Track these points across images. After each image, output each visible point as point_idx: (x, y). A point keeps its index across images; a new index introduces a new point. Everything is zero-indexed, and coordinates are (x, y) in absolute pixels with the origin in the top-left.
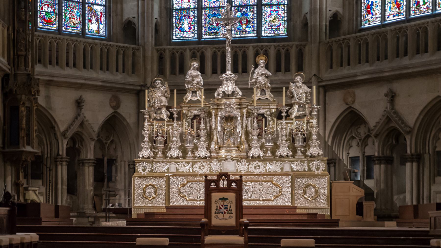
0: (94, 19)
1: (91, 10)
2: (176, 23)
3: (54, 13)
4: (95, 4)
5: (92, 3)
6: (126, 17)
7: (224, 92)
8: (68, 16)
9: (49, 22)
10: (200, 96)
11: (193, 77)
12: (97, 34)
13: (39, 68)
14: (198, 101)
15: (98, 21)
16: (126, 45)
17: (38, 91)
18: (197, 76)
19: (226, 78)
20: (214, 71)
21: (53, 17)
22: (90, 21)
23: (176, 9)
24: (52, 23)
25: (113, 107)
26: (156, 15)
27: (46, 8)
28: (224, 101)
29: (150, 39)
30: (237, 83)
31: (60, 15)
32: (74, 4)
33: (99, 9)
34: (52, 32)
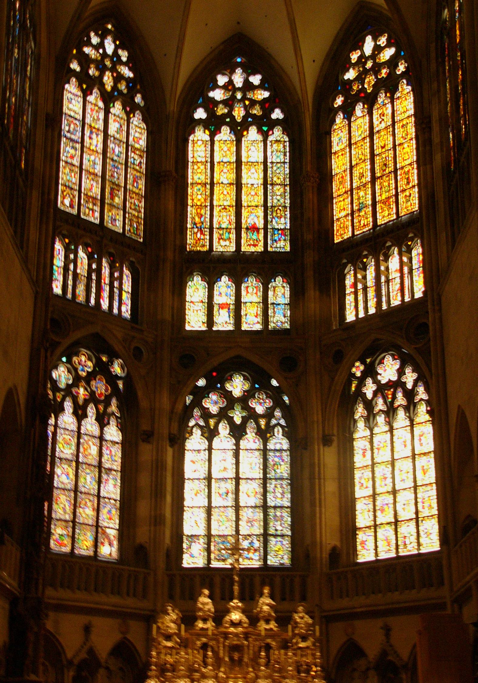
0: (106, 544)
1: (104, 533)
2: (187, 549)
3: (68, 535)
4: (109, 528)
5: (106, 527)
6: (138, 541)
7: (231, 621)
8: (81, 538)
9: (61, 545)
10: (210, 625)
11: (204, 604)
12: (109, 557)
13: (50, 592)
14: (207, 629)
15: (111, 544)
16: (136, 569)
17: (47, 615)
18: (207, 604)
19: (233, 607)
20: (223, 599)
21: (67, 541)
22: (103, 544)
23: (188, 536)
24: (65, 546)
25: (122, 633)
26: (167, 541)
27: (59, 531)
28: (232, 629)
29: (162, 564)
30: (244, 612)
31: (73, 538)
32: (87, 526)
33: (113, 533)
34: (65, 555)
